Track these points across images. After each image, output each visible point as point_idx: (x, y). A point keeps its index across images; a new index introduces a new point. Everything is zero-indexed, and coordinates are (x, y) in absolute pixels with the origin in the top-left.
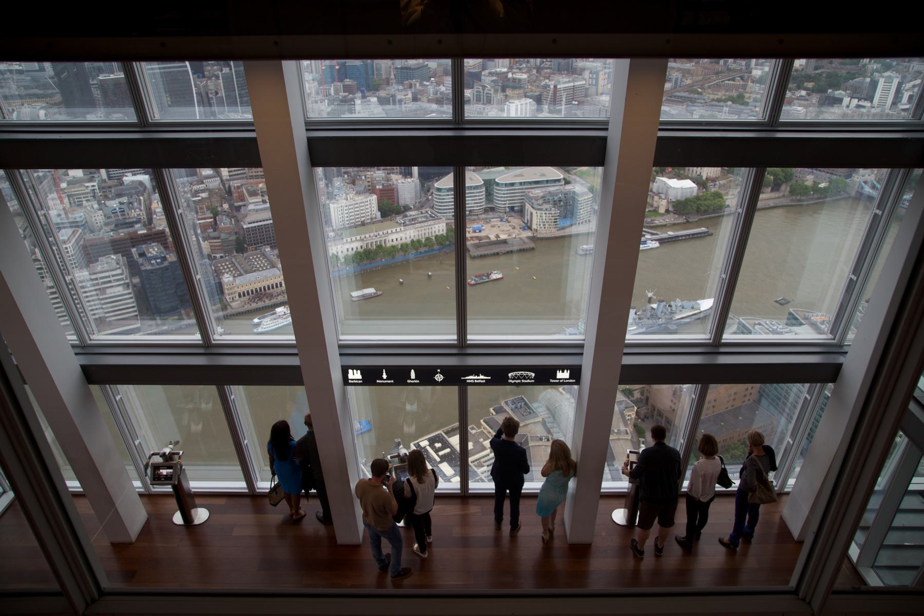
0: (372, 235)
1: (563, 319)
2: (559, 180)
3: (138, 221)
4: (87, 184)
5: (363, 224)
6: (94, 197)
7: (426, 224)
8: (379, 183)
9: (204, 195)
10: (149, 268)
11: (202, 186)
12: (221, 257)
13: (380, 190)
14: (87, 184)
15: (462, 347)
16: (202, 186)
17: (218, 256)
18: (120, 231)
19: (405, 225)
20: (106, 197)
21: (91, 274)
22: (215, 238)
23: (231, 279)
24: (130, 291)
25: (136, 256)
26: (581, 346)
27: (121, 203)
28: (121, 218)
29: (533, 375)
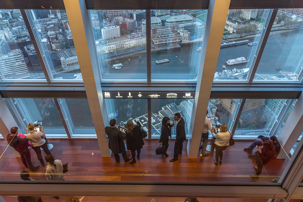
0: (118, 42)
1: (189, 73)
2: (191, 20)
3: (26, 36)
4: (4, 21)
5: (115, 38)
6: (7, 26)
7: (139, 38)
8: (121, 22)
9: (52, 26)
10: (32, 54)
11: (50, 22)
12: (60, 50)
13: (121, 24)
14: (4, 21)
15: (149, 84)
16: (50, 22)
17: (59, 50)
18: (19, 40)
19: (131, 38)
20: (12, 26)
21: (9, 57)
22: (57, 43)
23: (64, 59)
24: (25, 63)
25: (26, 50)
26: (196, 84)
27: (18, 28)
28: (19, 34)
29: (176, 95)
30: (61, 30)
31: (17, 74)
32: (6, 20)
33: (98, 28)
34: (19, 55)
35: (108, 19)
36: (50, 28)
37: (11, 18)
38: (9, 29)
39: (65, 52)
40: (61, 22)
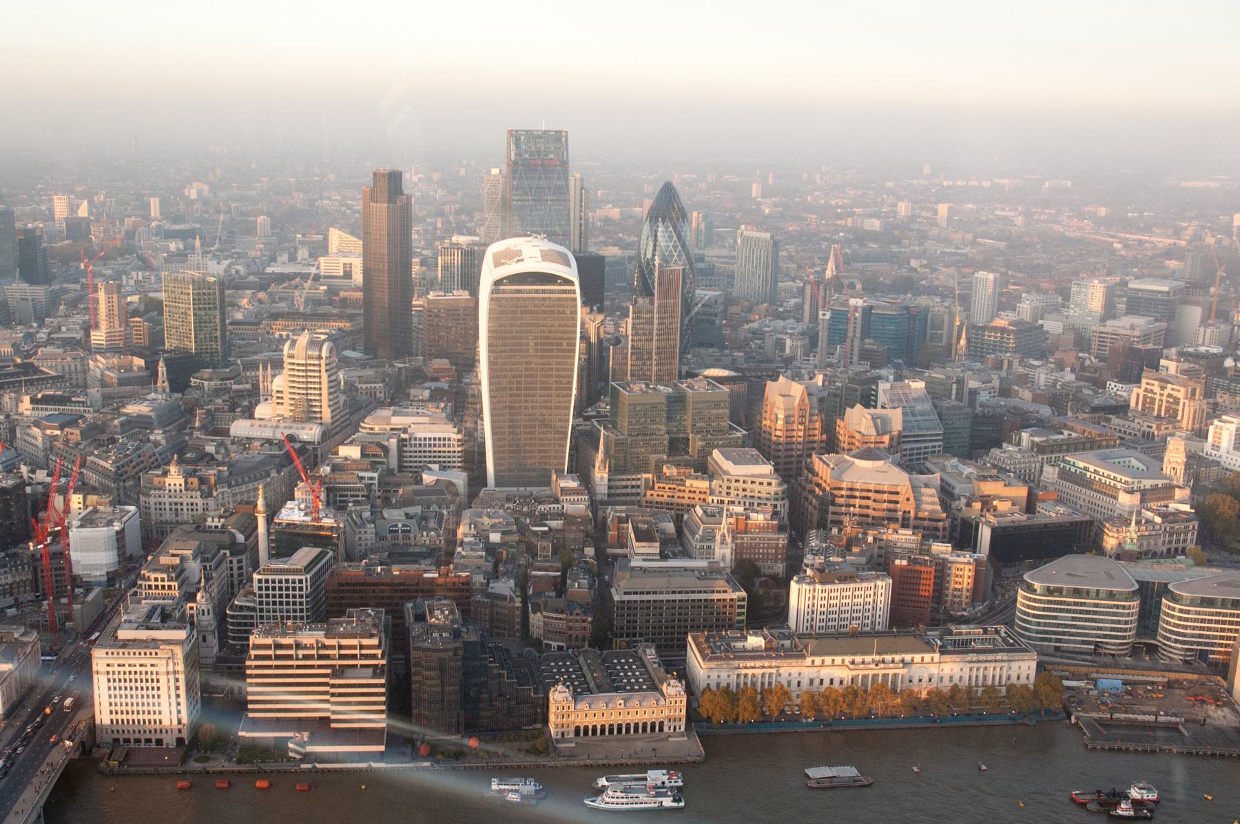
14: (362, 474)
17: (554, 644)
20: (387, 502)
21: (327, 637)
24: (383, 681)
30: (590, 551)
31: (333, 725)
32: (370, 474)
33: (780, 568)
34: (371, 636)
35: (840, 530)
36: (544, 532)
37: (393, 462)
38: (367, 514)
39: (581, 659)
40: (600, 513)
